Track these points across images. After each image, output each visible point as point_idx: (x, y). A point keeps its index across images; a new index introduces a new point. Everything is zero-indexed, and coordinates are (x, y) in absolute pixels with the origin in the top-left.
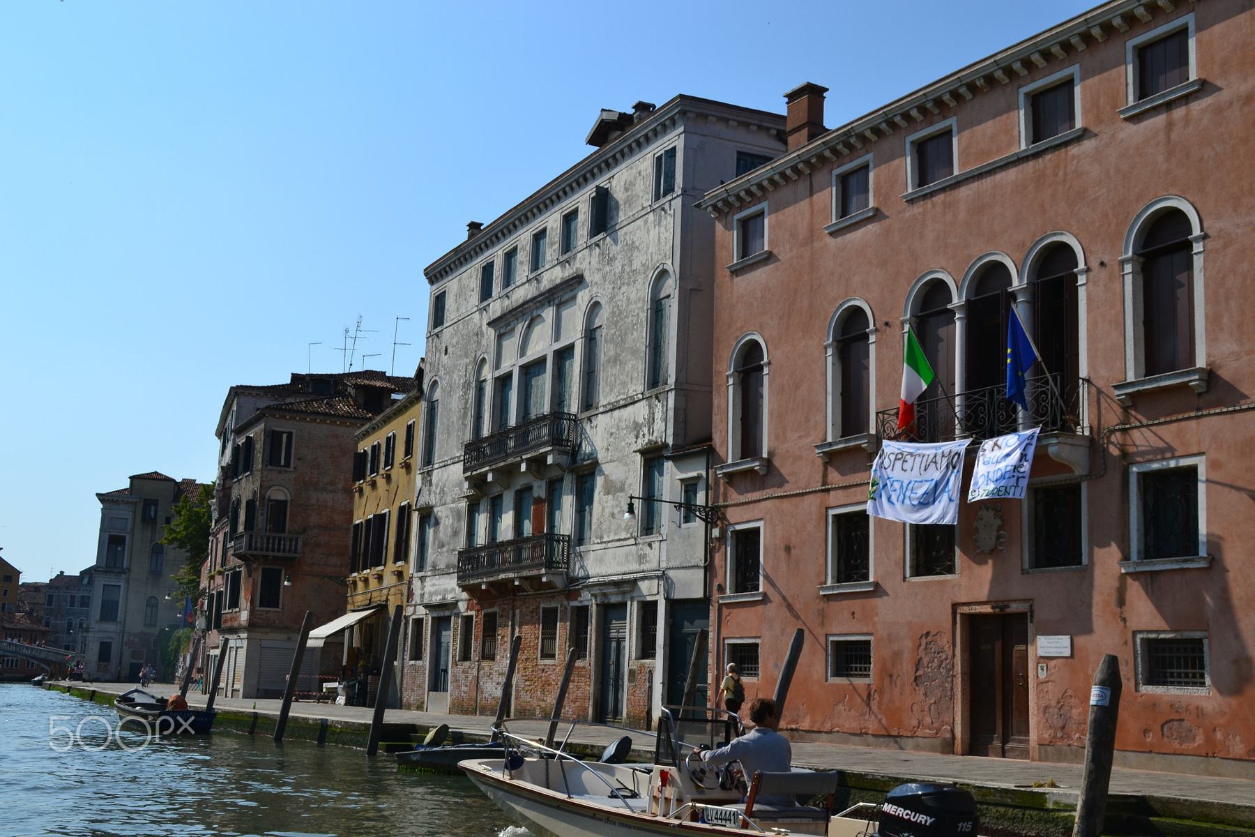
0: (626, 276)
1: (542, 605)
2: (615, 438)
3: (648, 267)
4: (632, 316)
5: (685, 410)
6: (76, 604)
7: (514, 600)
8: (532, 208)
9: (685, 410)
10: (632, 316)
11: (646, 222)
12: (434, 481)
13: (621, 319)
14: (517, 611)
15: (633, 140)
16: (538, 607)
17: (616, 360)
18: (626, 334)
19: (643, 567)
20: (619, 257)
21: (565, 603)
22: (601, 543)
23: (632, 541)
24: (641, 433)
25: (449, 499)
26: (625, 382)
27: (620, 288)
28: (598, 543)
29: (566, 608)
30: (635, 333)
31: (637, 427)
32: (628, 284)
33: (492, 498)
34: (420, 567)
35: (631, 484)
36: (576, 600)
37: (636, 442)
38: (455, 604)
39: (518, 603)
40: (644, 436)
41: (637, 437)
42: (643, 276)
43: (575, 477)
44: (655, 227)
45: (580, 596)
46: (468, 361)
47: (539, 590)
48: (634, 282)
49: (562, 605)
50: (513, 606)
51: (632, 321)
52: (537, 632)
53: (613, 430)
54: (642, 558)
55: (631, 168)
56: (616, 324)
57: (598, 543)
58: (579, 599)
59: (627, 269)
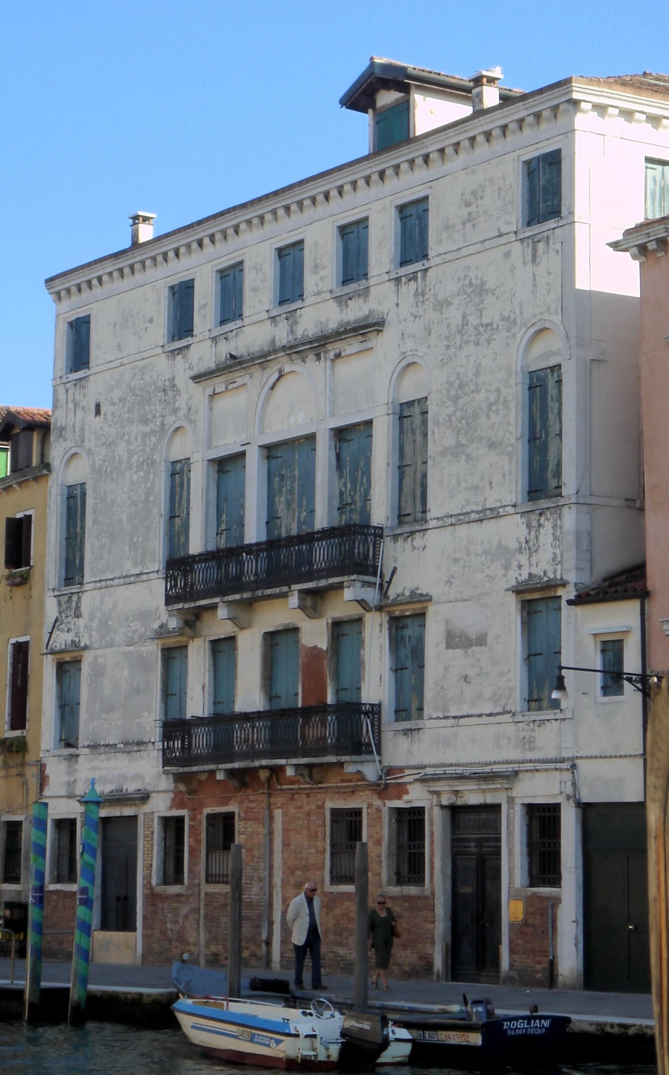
0: (470, 329)
1: (330, 805)
2: (464, 568)
3: (515, 322)
4: (487, 391)
5: (589, 533)
6: (385, 829)
7: (270, 795)
8: (190, 243)
9: (589, 533)
10: (487, 391)
11: (507, 255)
12: (85, 609)
13: (465, 395)
14: (278, 813)
15: (480, 130)
16: (322, 807)
17: (457, 451)
18: (475, 415)
19: (529, 756)
20: (456, 302)
21: (377, 802)
22: (446, 718)
23: (507, 718)
24: (515, 564)
25: (119, 638)
26: (477, 487)
27: (460, 348)
28: (438, 718)
29: (379, 810)
30: (493, 416)
31: (502, 554)
32: (477, 344)
33: (211, 641)
34: (68, 740)
35: (498, 636)
36: (399, 798)
37: (505, 575)
38: (144, 797)
39: (278, 800)
40: (520, 567)
41: (507, 567)
42: (505, 334)
43: (386, 619)
44: (525, 264)
45: (407, 793)
46: (148, 429)
47: (320, 783)
48: (489, 341)
49: (370, 806)
50: (269, 805)
51: (487, 398)
52: (320, 844)
53: (458, 555)
54: (528, 743)
55: (473, 172)
56: (455, 399)
57: (438, 718)
58: (405, 797)
59: (473, 320)
